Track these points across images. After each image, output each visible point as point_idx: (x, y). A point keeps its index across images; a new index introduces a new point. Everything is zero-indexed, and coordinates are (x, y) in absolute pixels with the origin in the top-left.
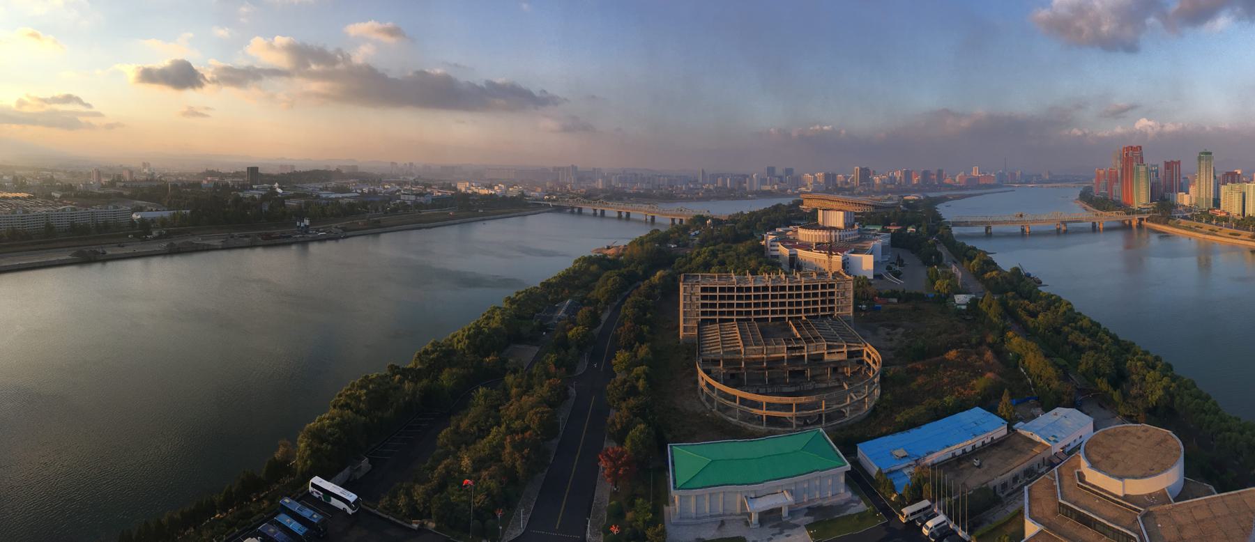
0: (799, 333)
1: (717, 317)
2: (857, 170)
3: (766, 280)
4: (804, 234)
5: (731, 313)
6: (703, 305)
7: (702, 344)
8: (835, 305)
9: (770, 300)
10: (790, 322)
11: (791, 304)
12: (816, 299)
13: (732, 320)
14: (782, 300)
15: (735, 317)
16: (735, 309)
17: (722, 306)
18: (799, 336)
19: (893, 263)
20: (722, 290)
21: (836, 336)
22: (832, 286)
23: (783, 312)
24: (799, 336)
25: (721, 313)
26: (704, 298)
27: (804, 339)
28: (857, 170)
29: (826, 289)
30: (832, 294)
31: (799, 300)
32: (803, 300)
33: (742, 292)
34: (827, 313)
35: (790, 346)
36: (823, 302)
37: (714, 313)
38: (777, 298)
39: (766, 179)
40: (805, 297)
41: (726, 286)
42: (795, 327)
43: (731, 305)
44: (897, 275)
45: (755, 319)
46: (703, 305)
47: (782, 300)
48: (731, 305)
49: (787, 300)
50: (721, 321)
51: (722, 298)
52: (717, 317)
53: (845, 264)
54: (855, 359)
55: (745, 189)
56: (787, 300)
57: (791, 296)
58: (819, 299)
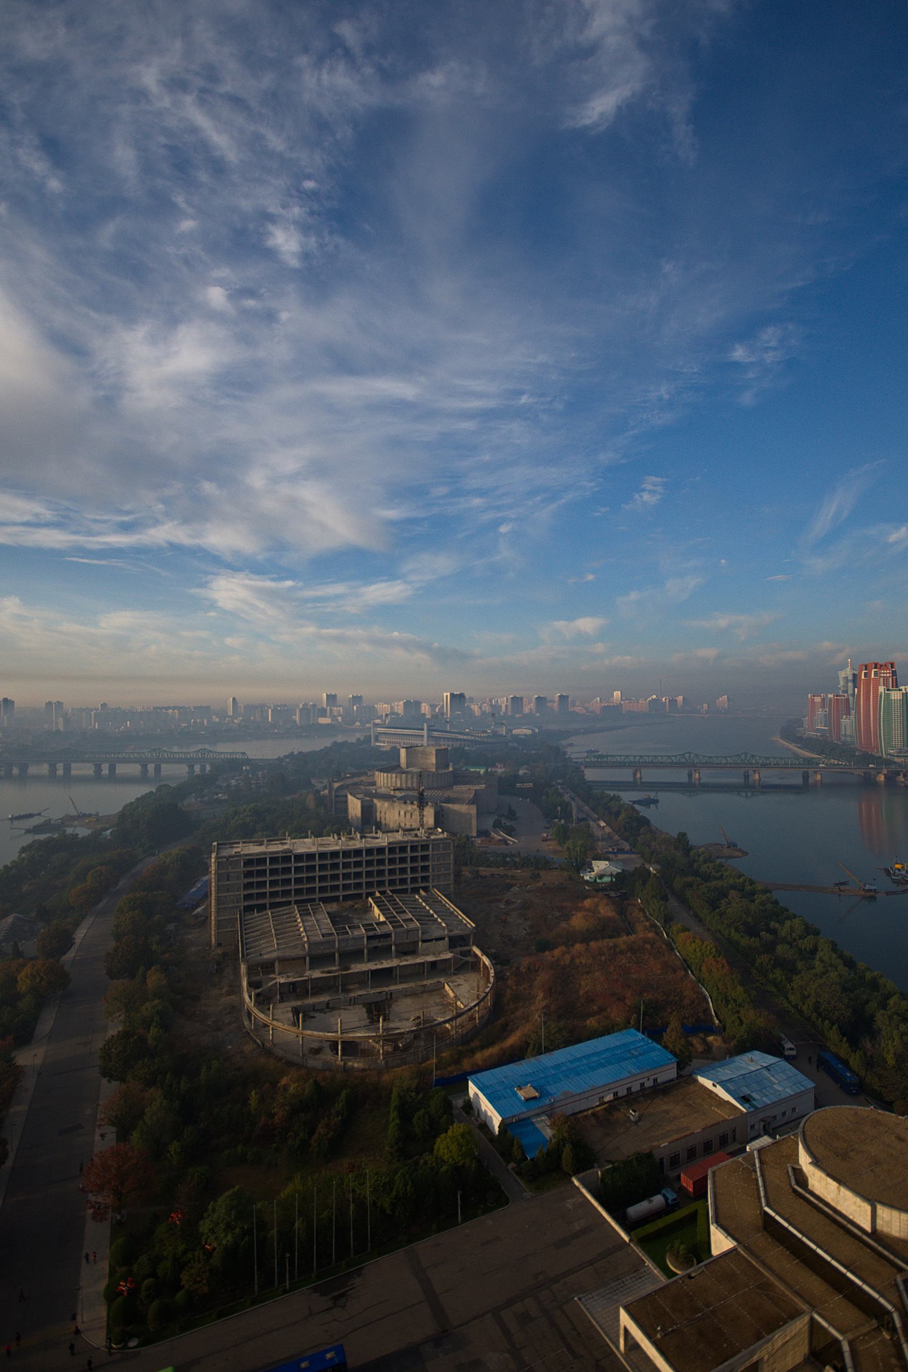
0: (384, 914)
1: (267, 901)
2: (447, 696)
3: (333, 843)
4: (383, 780)
5: (287, 893)
6: (248, 886)
7: (247, 944)
8: (430, 874)
9: (341, 871)
10: (370, 899)
11: (369, 874)
12: (405, 866)
13: (289, 903)
14: (358, 870)
15: (293, 899)
16: (293, 887)
17: (273, 883)
18: (382, 919)
19: (503, 815)
20: (274, 860)
21: (433, 916)
22: (425, 847)
23: (358, 886)
24: (382, 919)
25: (273, 894)
26: (248, 874)
27: (390, 922)
28: (447, 696)
29: (417, 851)
30: (425, 858)
31: (382, 868)
32: (387, 867)
33: (302, 861)
34: (418, 885)
35: (371, 933)
36: (413, 870)
37: (263, 895)
38: (350, 867)
39: (326, 709)
40: (389, 864)
41: (280, 855)
42: (378, 906)
43: (287, 882)
44: (510, 831)
45: (321, 899)
46: (248, 886)
47: (358, 870)
48: (288, 882)
49: (364, 869)
50: (273, 906)
51: (273, 872)
52: (267, 901)
53: (440, 818)
54: (459, 949)
55: (295, 722)
56: (364, 869)
57: (369, 863)
58: (408, 865)
